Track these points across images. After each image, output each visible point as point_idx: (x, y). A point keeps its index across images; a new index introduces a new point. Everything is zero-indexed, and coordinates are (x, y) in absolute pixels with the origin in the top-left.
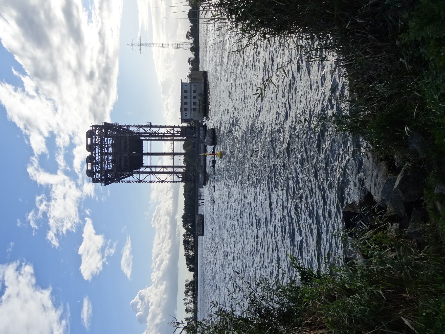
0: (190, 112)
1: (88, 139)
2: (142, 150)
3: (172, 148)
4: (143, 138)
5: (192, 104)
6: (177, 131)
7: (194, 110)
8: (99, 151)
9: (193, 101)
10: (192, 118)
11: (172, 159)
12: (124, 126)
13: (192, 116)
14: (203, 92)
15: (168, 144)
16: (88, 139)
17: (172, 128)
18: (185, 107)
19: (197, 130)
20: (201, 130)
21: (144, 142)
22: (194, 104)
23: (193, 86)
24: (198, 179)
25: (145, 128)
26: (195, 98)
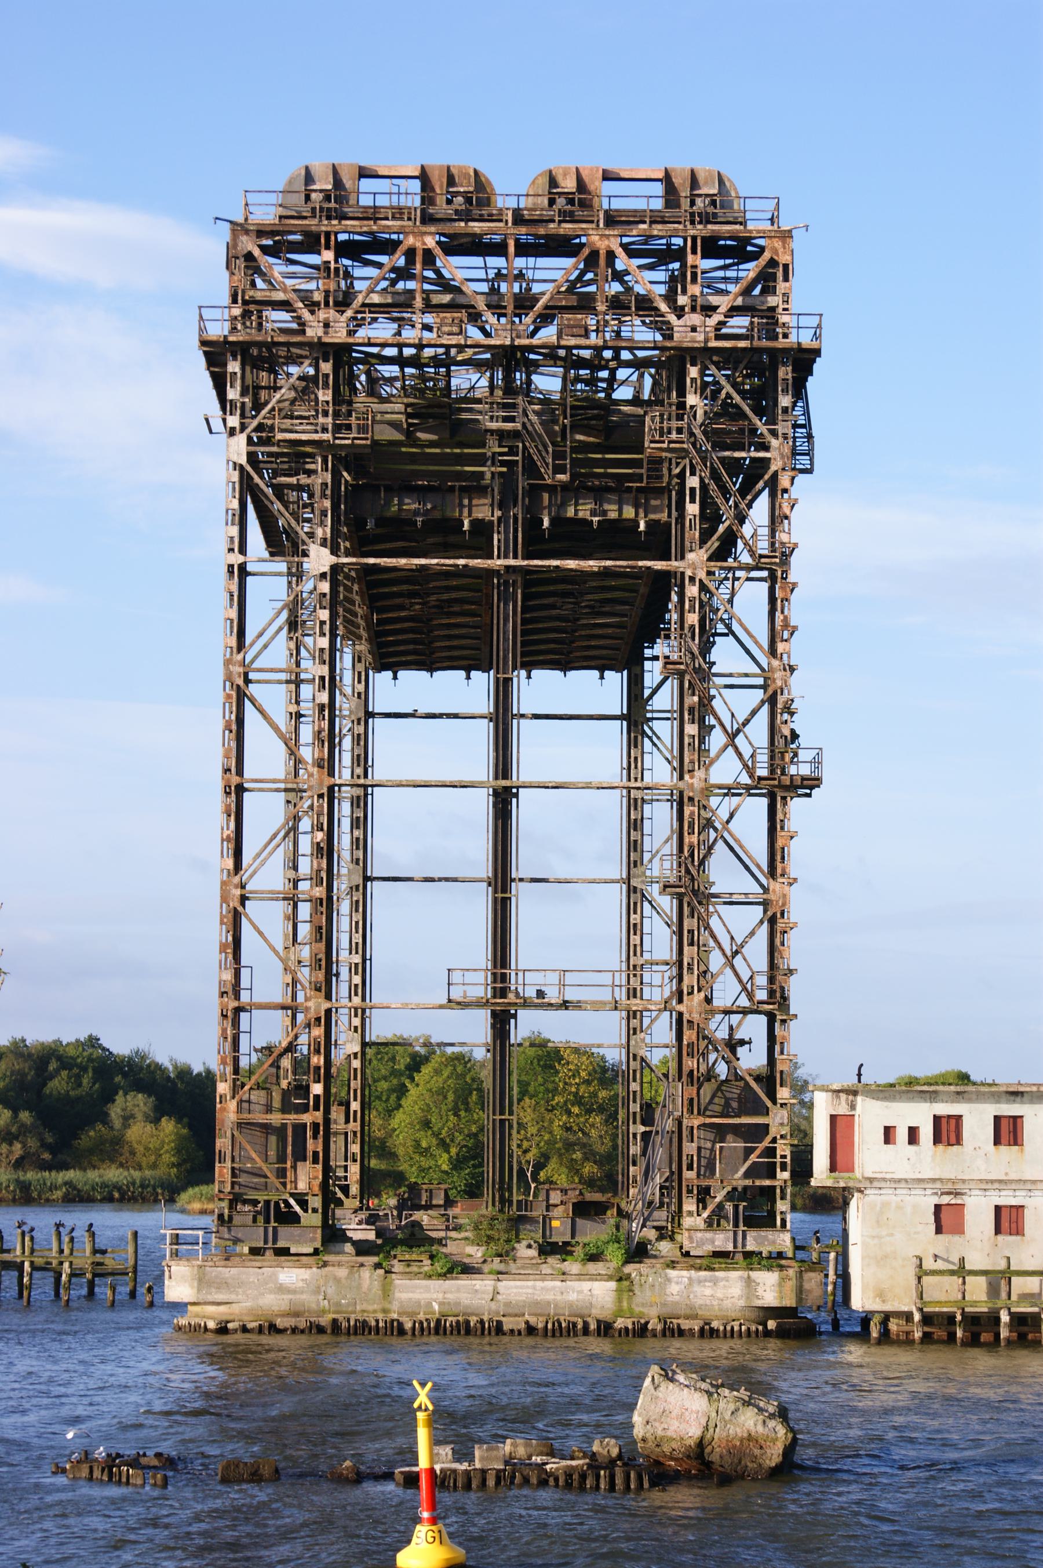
2: (529, 666)
3: (571, 995)
4: (653, 673)
5: (1007, 1199)
6: (733, 1045)
8: (536, 288)
11: (457, 994)
12: (777, 519)
13: (888, 1196)
17: (762, 995)
21: (615, 681)
25: (758, 732)
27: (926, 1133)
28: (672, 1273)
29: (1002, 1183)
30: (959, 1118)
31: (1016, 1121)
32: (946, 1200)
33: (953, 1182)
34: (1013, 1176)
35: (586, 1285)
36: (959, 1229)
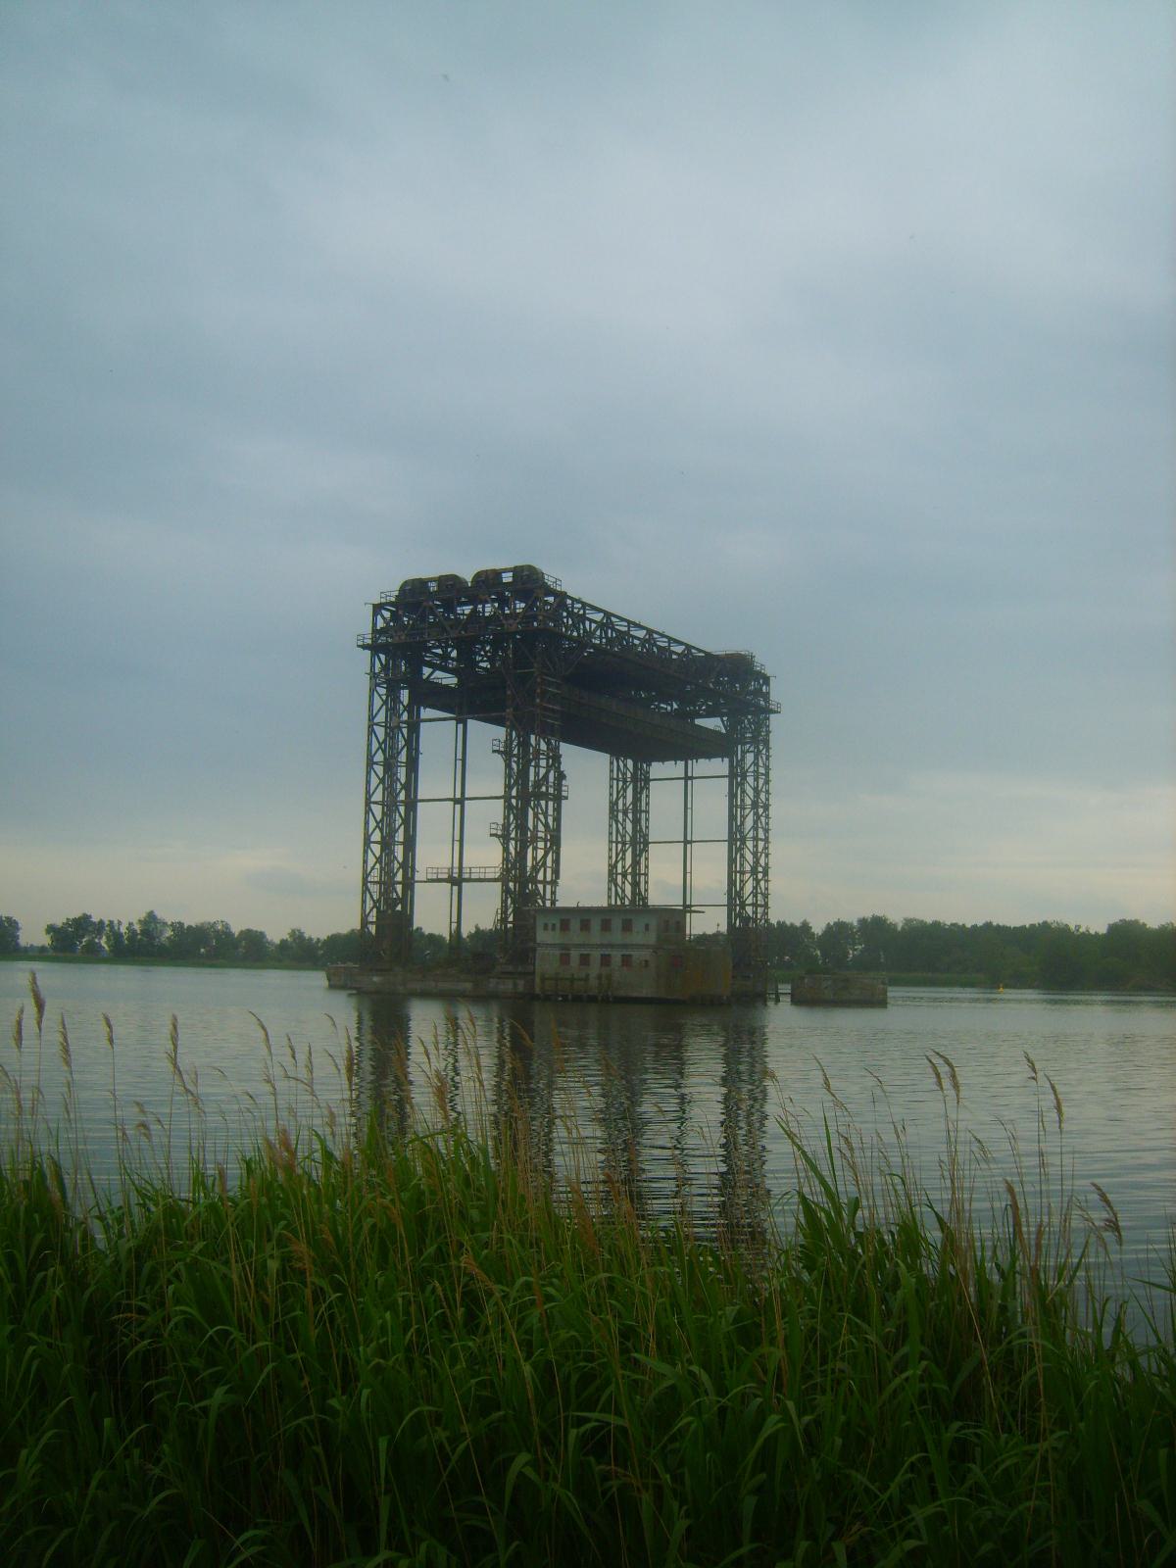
0: (557, 942)
1: (511, 574)
7: (565, 959)
10: (540, 951)
11: (430, 877)
14: (622, 993)
15: (486, 856)
16: (511, 574)
18: (575, 925)
19: (520, 969)
20: (515, 985)
22: (585, 960)
23: (646, 954)
26: (606, 960)
27: (558, 925)
28: (491, 980)
30: (631, 920)
31: (588, 921)
34: (587, 942)
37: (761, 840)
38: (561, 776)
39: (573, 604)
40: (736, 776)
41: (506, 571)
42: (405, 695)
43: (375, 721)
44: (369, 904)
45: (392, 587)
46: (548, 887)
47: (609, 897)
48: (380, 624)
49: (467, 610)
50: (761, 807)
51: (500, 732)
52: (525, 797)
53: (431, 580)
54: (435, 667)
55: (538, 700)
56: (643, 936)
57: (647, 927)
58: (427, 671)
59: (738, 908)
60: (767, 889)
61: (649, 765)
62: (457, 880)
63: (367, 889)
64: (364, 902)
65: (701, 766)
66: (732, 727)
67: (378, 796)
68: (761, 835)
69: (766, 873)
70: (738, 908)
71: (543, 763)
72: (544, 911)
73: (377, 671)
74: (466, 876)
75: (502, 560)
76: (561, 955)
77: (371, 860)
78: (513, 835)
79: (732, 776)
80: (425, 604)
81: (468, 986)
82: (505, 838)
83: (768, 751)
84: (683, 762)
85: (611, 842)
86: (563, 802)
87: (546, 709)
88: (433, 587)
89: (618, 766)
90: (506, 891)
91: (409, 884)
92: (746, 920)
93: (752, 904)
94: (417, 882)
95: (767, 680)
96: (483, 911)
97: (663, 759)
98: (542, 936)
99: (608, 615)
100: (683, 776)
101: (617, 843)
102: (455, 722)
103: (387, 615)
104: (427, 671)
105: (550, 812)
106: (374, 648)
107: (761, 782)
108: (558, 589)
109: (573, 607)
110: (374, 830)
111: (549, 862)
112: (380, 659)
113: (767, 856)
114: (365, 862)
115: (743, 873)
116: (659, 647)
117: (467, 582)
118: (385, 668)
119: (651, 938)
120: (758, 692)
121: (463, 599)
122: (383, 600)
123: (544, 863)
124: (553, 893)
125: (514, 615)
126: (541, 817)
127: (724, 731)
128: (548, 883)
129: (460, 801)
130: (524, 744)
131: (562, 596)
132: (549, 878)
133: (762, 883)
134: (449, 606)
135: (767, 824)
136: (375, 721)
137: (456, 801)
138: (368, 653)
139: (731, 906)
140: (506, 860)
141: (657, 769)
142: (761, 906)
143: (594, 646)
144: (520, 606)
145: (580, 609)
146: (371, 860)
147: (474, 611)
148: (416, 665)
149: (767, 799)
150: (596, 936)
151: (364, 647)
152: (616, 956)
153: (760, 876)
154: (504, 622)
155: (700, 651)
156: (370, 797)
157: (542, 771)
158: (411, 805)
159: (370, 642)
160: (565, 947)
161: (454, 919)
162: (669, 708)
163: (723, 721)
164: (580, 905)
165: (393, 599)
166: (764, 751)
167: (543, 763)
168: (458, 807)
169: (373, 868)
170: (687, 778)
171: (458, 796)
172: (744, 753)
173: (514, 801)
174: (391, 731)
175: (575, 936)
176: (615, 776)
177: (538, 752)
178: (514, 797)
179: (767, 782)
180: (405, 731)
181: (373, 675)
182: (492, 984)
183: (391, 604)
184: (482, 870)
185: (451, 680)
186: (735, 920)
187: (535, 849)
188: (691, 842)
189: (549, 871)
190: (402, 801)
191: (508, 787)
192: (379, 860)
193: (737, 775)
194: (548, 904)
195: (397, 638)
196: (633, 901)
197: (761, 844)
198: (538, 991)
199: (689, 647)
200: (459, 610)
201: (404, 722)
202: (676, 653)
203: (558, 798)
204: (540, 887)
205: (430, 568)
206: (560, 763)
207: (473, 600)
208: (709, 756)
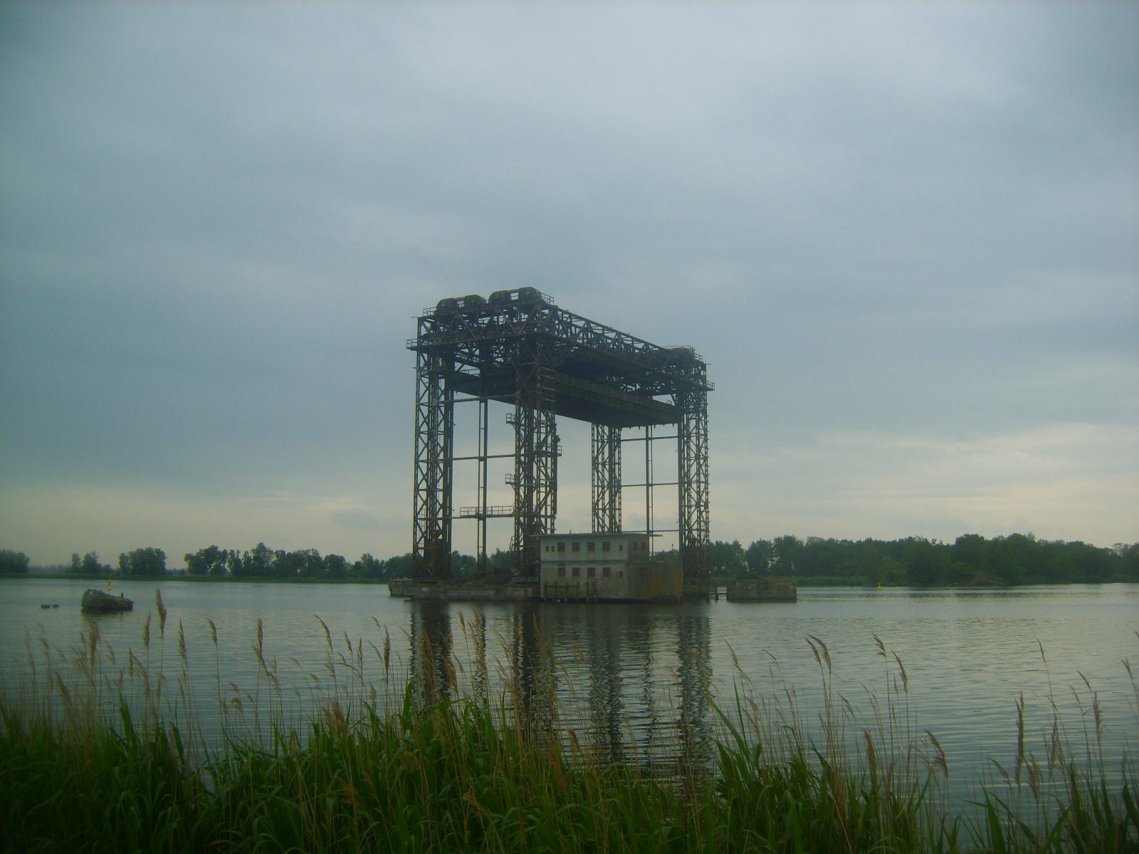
0: (557, 559)
5: (576, 566)
7: (562, 572)
9: (584, 569)
10: (543, 567)
11: (462, 514)
14: (604, 596)
15: (502, 498)
18: (568, 547)
19: (529, 580)
20: (526, 591)
22: (576, 572)
24: (421, 583)
26: (591, 572)
27: (556, 549)
28: (508, 588)
29: (574, 562)
32: (561, 567)
33: (562, 561)
35: (489, 592)
36: (564, 574)
37: (703, 482)
38: (556, 439)
39: (562, 315)
40: (683, 437)
41: (514, 291)
42: (442, 383)
43: (421, 402)
44: (419, 535)
45: (431, 305)
46: (549, 520)
47: (594, 526)
48: (424, 332)
49: (486, 320)
50: (701, 459)
51: (511, 409)
52: (531, 455)
53: (460, 299)
54: (464, 362)
55: (539, 385)
56: (618, 554)
57: (621, 548)
58: (458, 365)
59: (687, 532)
60: (707, 518)
61: (620, 430)
62: (482, 517)
63: (418, 524)
64: (415, 533)
65: (658, 430)
66: (681, 400)
67: (424, 456)
68: (702, 479)
69: (706, 506)
70: (687, 532)
71: (543, 430)
72: (546, 537)
73: (421, 366)
74: (489, 513)
75: (511, 284)
76: (559, 569)
77: (420, 503)
78: (522, 483)
79: (680, 436)
80: (455, 316)
81: (492, 593)
82: (517, 485)
83: (706, 418)
84: (645, 427)
85: (593, 486)
86: (558, 458)
87: (544, 391)
88: (461, 304)
89: (598, 430)
90: (518, 524)
91: (447, 520)
92: (693, 541)
93: (697, 530)
94: (454, 518)
95: (704, 367)
96: (502, 538)
97: (630, 426)
98: (545, 555)
99: (588, 322)
100: (645, 437)
101: (598, 486)
102: (478, 402)
103: (428, 325)
104: (458, 365)
105: (549, 465)
106: (419, 349)
107: (701, 440)
108: (552, 304)
109: (563, 317)
110: (422, 481)
111: (549, 502)
112: (424, 358)
113: (707, 494)
114: (415, 504)
115: (690, 507)
116: (625, 345)
117: (485, 301)
118: (427, 364)
119: (624, 556)
120: (698, 375)
121: (483, 313)
122: (425, 315)
123: (546, 503)
124: (552, 524)
125: (520, 323)
126: (543, 469)
127: (673, 404)
128: (549, 517)
129: (484, 459)
130: (529, 417)
131: (554, 309)
132: (549, 514)
133: (704, 514)
134: (473, 318)
135: (706, 471)
136: (421, 402)
137: (480, 459)
138: (415, 353)
139: (681, 532)
140: (517, 501)
141: (626, 433)
142: (704, 530)
143: (578, 345)
144: (524, 317)
145: (567, 318)
146: (420, 503)
147: (491, 321)
148: (450, 360)
149: (706, 453)
150: (584, 554)
151: (412, 349)
152: (599, 569)
153: (702, 508)
154: (513, 328)
155: (655, 346)
156: (419, 457)
157: (543, 436)
158: (448, 462)
159: (416, 345)
160: (562, 563)
161: (481, 544)
162: (634, 388)
163: (673, 397)
164: (572, 533)
165: (432, 314)
166: (703, 418)
167: (543, 430)
168: (482, 463)
169: (421, 509)
170: (647, 439)
171: (482, 455)
172: (688, 420)
173: (522, 458)
174: (433, 409)
175: (569, 554)
176: (596, 438)
177: (539, 422)
178: (523, 455)
179: (706, 440)
180: (443, 409)
181: (419, 369)
182: (509, 591)
183: (430, 317)
184: (501, 509)
185: (475, 372)
186: (685, 542)
187: (539, 492)
188: (652, 485)
189: (549, 508)
190: (441, 460)
191: (518, 448)
192: (425, 503)
193: (683, 437)
194: (549, 532)
195: (435, 342)
196: (610, 528)
197: (702, 486)
198: (542, 596)
199: (647, 344)
200: (480, 321)
201: (442, 403)
202: (638, 349)
203: (555, 455)
204: (543, 520)
205: (458, 290)
206: (555, 430)
207: (490, 313)
208: (663, 423)
